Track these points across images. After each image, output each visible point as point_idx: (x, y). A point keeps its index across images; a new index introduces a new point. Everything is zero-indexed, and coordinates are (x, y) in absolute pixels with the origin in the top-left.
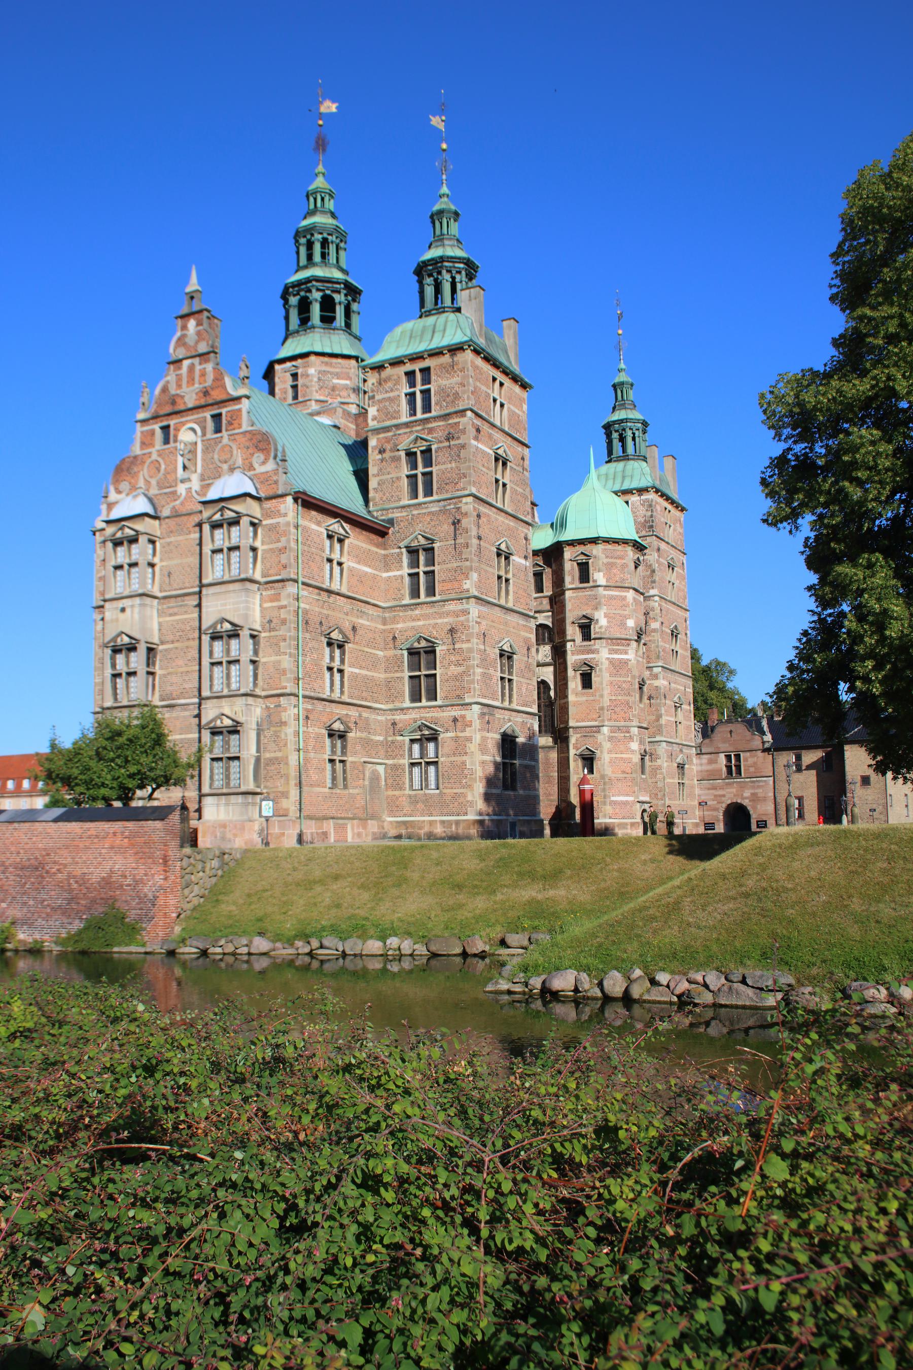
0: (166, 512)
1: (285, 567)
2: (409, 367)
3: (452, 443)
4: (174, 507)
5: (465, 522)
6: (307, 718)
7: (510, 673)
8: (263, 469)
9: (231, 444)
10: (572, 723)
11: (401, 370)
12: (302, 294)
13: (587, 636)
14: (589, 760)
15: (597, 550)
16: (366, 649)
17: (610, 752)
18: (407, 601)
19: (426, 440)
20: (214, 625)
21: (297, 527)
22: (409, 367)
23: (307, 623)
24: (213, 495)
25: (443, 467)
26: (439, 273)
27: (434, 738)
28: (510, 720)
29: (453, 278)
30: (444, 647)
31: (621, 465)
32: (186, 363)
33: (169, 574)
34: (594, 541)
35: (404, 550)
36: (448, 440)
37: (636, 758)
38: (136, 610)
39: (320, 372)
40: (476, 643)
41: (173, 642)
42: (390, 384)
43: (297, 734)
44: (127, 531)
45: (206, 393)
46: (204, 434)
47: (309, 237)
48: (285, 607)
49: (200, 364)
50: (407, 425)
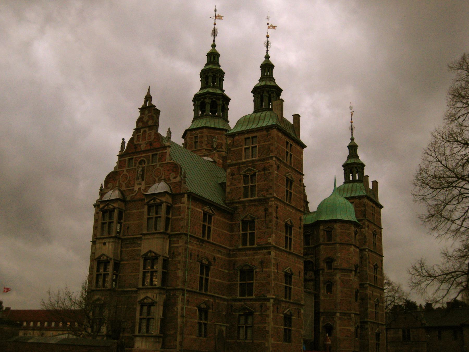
0: (128, 199)
1: (182, 227)
2: (246, 136)
3: (266, 172)
4: (132, 196)
5: (270, 210)
6: (188, 301)
7: (290, 284)
8: (174, 181)
9: (160, 168)
10: (321, 310)
12: (202, 100)
13: (330, 267)
14: (329, 329)
15: (336, 226)
16: (220, 269)
17: (340, 325)
18: (241, 247)
19: (254, 171)
21: (188, 208)
22: (246, 136)
23: (191, 255)
24: (151, 191)
25: (262, 183)
26: (263, 92)
27: (251, 314)
28: (288, 308)
29: (270, 95)
30: (257, 270)
31: (351, 185)
32: (142, 130)
33: (128, 228)
34: (336, 221)
35: (241, 222)
37: (353, 329)
38: (111, 244)
40: (273, 269)
41: (127, 260)
43: (182, 308)
44: (110, 206)
45: (151, 144)
46: (148, 163)
47: (207, 74)
48: (181, 246)
49: (149, 131)
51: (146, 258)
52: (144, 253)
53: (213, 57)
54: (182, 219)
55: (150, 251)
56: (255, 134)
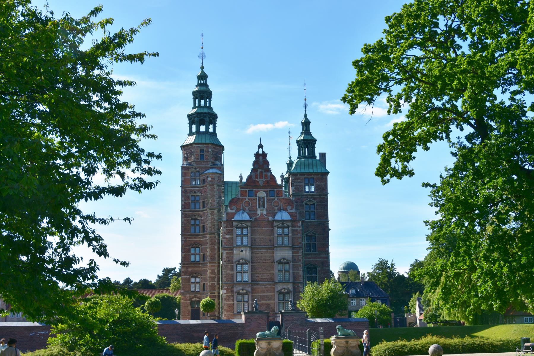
2: (306, 176)
8: (291, 211)
11: (304, 177)
12: (202, 117)
20: (280, 260)
22: (306, 176)
32: (259, 170)
33: (255, 240)
36: (321, 202)
39: (213, 151)
42: (299, 181)
45: (268, 182)
46: (267, 196)
50: (306, 195)
51: (280, 262)
52: (278, 259)
53: (203, 77)
54: (299, 238)
55: (284, 259)
56: (313, 176)
